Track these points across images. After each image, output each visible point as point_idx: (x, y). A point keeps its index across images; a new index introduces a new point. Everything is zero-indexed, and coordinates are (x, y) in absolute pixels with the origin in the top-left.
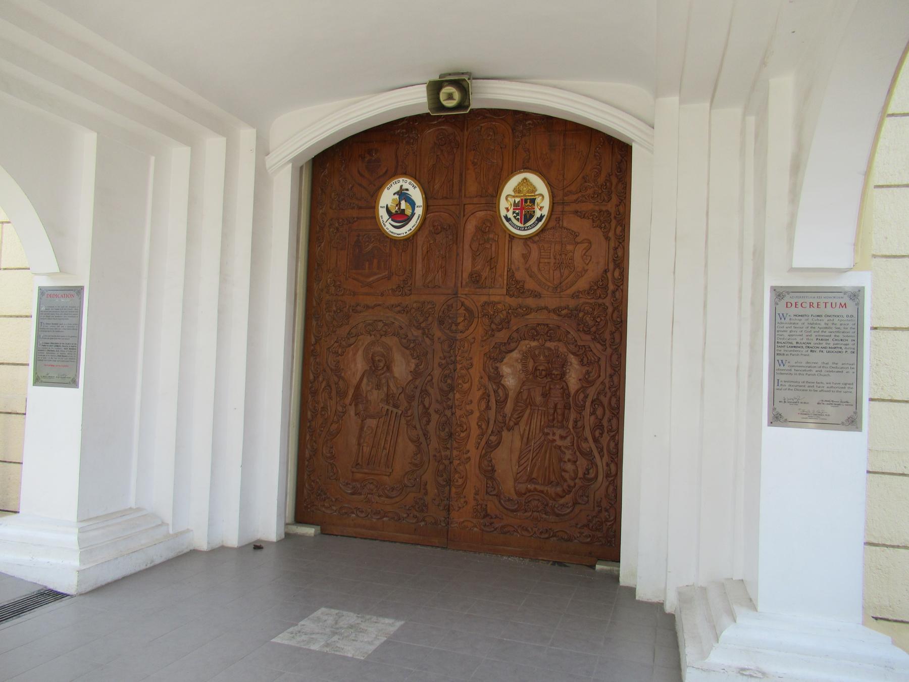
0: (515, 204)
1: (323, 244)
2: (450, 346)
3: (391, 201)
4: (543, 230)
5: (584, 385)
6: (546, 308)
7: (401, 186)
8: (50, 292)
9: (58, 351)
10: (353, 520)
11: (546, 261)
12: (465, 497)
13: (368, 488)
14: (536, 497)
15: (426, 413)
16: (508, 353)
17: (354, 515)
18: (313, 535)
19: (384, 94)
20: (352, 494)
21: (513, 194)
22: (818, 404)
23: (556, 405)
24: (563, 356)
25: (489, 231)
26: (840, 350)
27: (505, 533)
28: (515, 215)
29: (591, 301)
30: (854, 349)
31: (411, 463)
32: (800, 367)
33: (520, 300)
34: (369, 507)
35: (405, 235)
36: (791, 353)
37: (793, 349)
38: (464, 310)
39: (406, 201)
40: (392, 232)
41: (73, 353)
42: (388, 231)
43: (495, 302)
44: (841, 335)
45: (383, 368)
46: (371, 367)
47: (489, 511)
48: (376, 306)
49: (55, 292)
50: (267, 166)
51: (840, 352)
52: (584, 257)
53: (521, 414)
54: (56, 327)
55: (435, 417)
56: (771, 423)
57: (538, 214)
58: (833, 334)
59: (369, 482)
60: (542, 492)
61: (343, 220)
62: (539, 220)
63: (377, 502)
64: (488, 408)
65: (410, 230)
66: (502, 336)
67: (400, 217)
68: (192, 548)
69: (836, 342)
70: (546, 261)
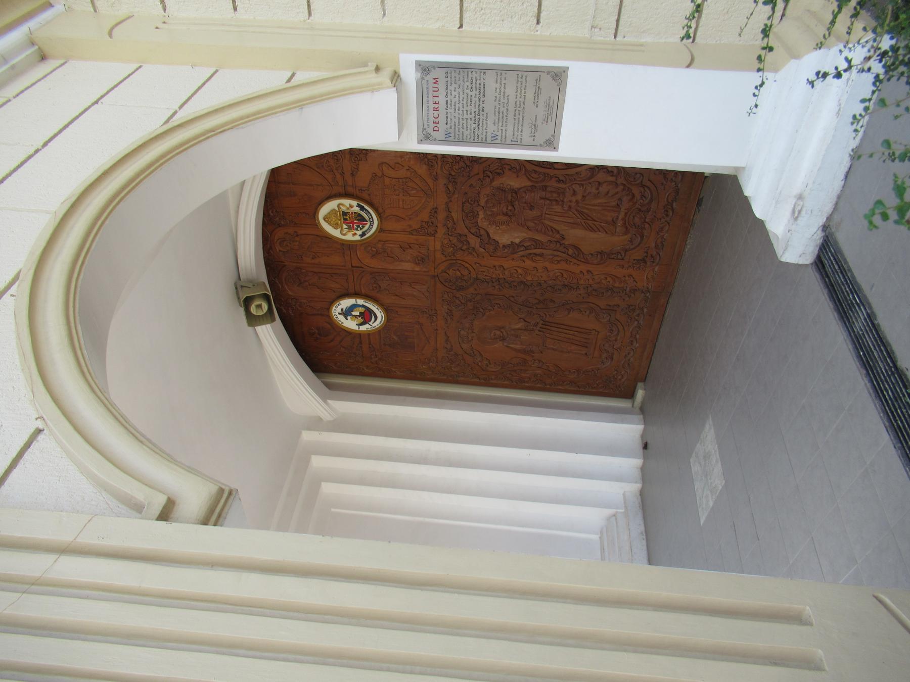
1: (393, 369)
3: (353, 322)
5: (523, 172)
6: (447, 203)
7: (339, 313)
11: (401, 203)
12: (624, 276)
14: (631, 217)
18: (644, 392)
20: (612, 359)
21: (339, 230)
22: (537, 107)
23: (541, 198)
24: (493, 191)
25: (375, 248)
26: (482, 85)
27: (663, 245)
28: (359, 229)
29: (440, 163)
30: (481, 72)
31: (588, 316)
32: (499, 122)
35: (382, 313)
36: (484, 129)
37: (480, 128)
39: (352, 311)
40: (381, 322)
42: (379, 325)
43: (441, 246)
44: (466, 84)
45: (502, 332)
46: (500, 341)
47: (640, 258)
50: (332, 419)
51: (484, 85)
52: (396, 169)
53: (549, 228)
56: (555, 149)
57: (357, 209)
58: (466, 91)
60: (626, 214)
61: (371, 355)
62: (362, 208)
63: (622, 342)
64: (541, 255)
65: (378, 309)
66: (474, 241)
67: (367, 316)
68: (638, 494)
69: (474, 88)
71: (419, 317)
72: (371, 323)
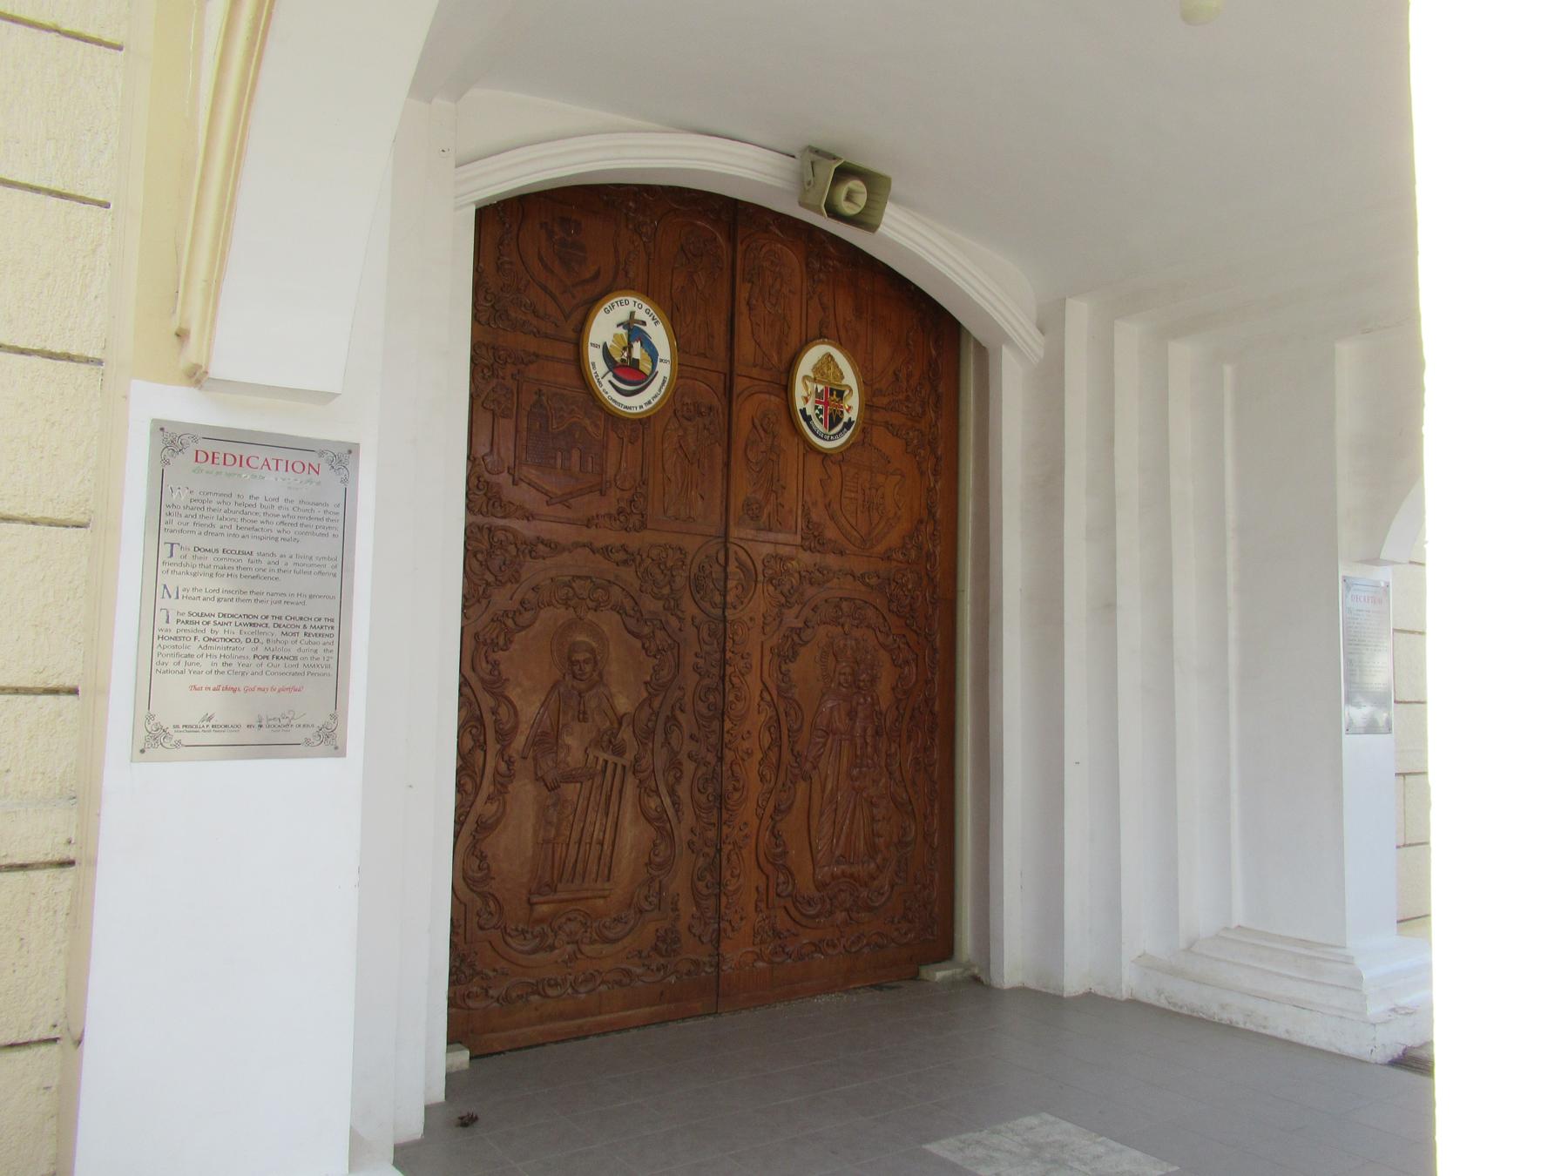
0: (818, 395)
2: (712, 634)
3: (612, 338)
4: (850, 447)
5: (899, 697)
7: (632, 314)
8: (210, 447)
9: (257, 641)
10: (536, 1009)
11: (853, 495)
13: (567, 930)
15: (675, 764)
16: (801, 645)
17: (537, 997)
18: (466, 1066)
19: (694, 136)
21: (812, 375)
23: (865, 730)
28: (817, 411)
33: (818, 557)
34: (570, 970)
35: (639, 410)
38: (737, 567)
39: (641, 345)
40: (615, 402)
41: (321, 648)
42: (606, 396)
48: (577, 545)
49: (237, 450)
54: (245, 564)
55: (689, 767)
57: (845, 419)
59: (569, 920)
60: (852, 876)
65: (649, 402)
70: (853, 495)
71: (623, 490)
72: (610, 376)
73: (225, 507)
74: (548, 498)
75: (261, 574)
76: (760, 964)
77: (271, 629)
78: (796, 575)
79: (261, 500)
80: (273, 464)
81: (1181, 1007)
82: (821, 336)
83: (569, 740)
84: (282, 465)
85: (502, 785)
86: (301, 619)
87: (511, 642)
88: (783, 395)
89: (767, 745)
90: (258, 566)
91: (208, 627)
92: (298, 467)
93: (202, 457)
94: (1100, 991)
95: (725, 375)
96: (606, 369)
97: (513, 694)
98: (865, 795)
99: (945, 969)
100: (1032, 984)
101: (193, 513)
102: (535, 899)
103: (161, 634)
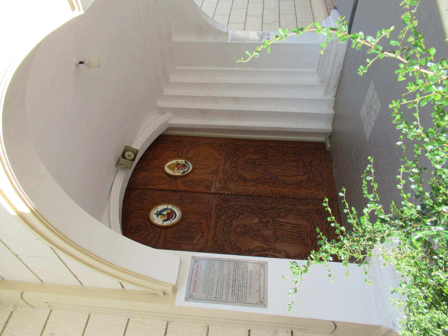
0: (178, 169)
4: (192, 162)
7: (155, 214)
8: (192, 289)
9: (239, 280)
16: (243, 176)
21: (173, 171)
35: (180, 213)
40: (178, 219)
41: (241, 266)
54: (220, 282)
59: (312, 235)
60: (303, 166)
65: (178, 211)
71: (201, 218)
72: (171, 220)
73: (206, 286)
74: (202, 237)
75: (223, 278)
76: (325, 189)
77: (236, 276)
78: (224, 177)
79: (205, 278)
80: (196, 275)
81: (337, 85)
82: (163, 168)
83: (265, 234)
84: (197, 273)
85: (276, 251)
86: (234, 270)
87: (239, 247)
88: (178, 178)
89: (268, 186)
90: (221, 279)
91: (235, 290)
92: (197, 269)
93: (194, 290)
94: (333, 105)
95: (172, 192)
96: (169, 221)
97: (253, 247)
98: (282, 162)
99: (327, 144)
100: (331, 122)
101: (207, 293)
102: (307, 244)
103: (237, 301)
